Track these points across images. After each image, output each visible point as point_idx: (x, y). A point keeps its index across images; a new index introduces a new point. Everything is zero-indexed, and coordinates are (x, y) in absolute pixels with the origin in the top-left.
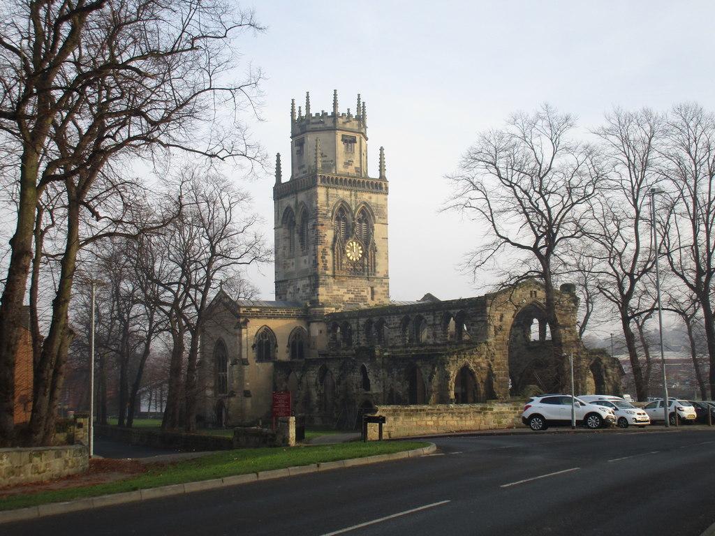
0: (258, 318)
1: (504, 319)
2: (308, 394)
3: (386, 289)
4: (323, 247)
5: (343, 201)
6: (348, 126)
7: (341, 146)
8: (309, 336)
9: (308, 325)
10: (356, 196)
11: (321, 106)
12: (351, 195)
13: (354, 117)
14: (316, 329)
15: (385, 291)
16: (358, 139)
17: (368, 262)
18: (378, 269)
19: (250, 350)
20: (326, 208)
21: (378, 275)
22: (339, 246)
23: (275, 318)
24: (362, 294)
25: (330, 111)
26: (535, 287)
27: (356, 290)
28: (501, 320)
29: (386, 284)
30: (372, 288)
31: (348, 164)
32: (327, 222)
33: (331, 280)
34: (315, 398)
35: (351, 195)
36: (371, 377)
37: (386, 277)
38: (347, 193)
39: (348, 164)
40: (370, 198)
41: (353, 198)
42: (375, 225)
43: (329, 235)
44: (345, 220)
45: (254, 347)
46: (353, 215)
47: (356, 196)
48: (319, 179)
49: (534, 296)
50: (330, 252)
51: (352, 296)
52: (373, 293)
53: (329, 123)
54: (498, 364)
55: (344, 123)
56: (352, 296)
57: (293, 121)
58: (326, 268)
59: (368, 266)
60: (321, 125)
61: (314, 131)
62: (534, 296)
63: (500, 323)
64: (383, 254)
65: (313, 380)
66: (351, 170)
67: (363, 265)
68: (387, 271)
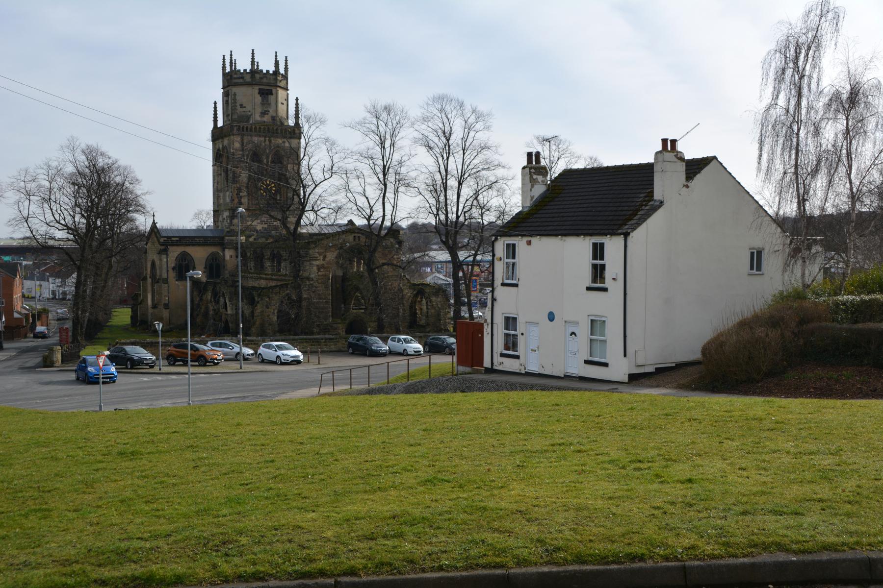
0: (177, 245)
1: (327, 259)
2: (207, 308)
6: (265, 80)
7: (258, 99)
8: (224, 259)
9: (223, 250)
10: (270, 141)
11: (244, 65)
13: (271, 72)
14: (228, 254)
16: (274, 92)
19: (171, 271)
22: (253, 186)
23: (193, 245)
25: (248, 69)
28: (324, 260)
31: (264, 113)
34: (211, 313)
36: (227, 301)
38: (262, 139)
39: (264, 113)
41: (267, 143)
43: (244, 176)
44: (260, 161)
45: (173, 269)
46: (267, 158)
47: (270, 141)
48: (235, 129)
49: (357, 240)
51: (266, 226)
54: (319, 295)
55: (261, 78)
56: (266, 226)
57: (225, 75)
60: (241, 80)
61: (236, 85)
62: (357, 240)
63: (322, 262)
65: (209, 297)
66: (266, 118)
67: (276, 199)
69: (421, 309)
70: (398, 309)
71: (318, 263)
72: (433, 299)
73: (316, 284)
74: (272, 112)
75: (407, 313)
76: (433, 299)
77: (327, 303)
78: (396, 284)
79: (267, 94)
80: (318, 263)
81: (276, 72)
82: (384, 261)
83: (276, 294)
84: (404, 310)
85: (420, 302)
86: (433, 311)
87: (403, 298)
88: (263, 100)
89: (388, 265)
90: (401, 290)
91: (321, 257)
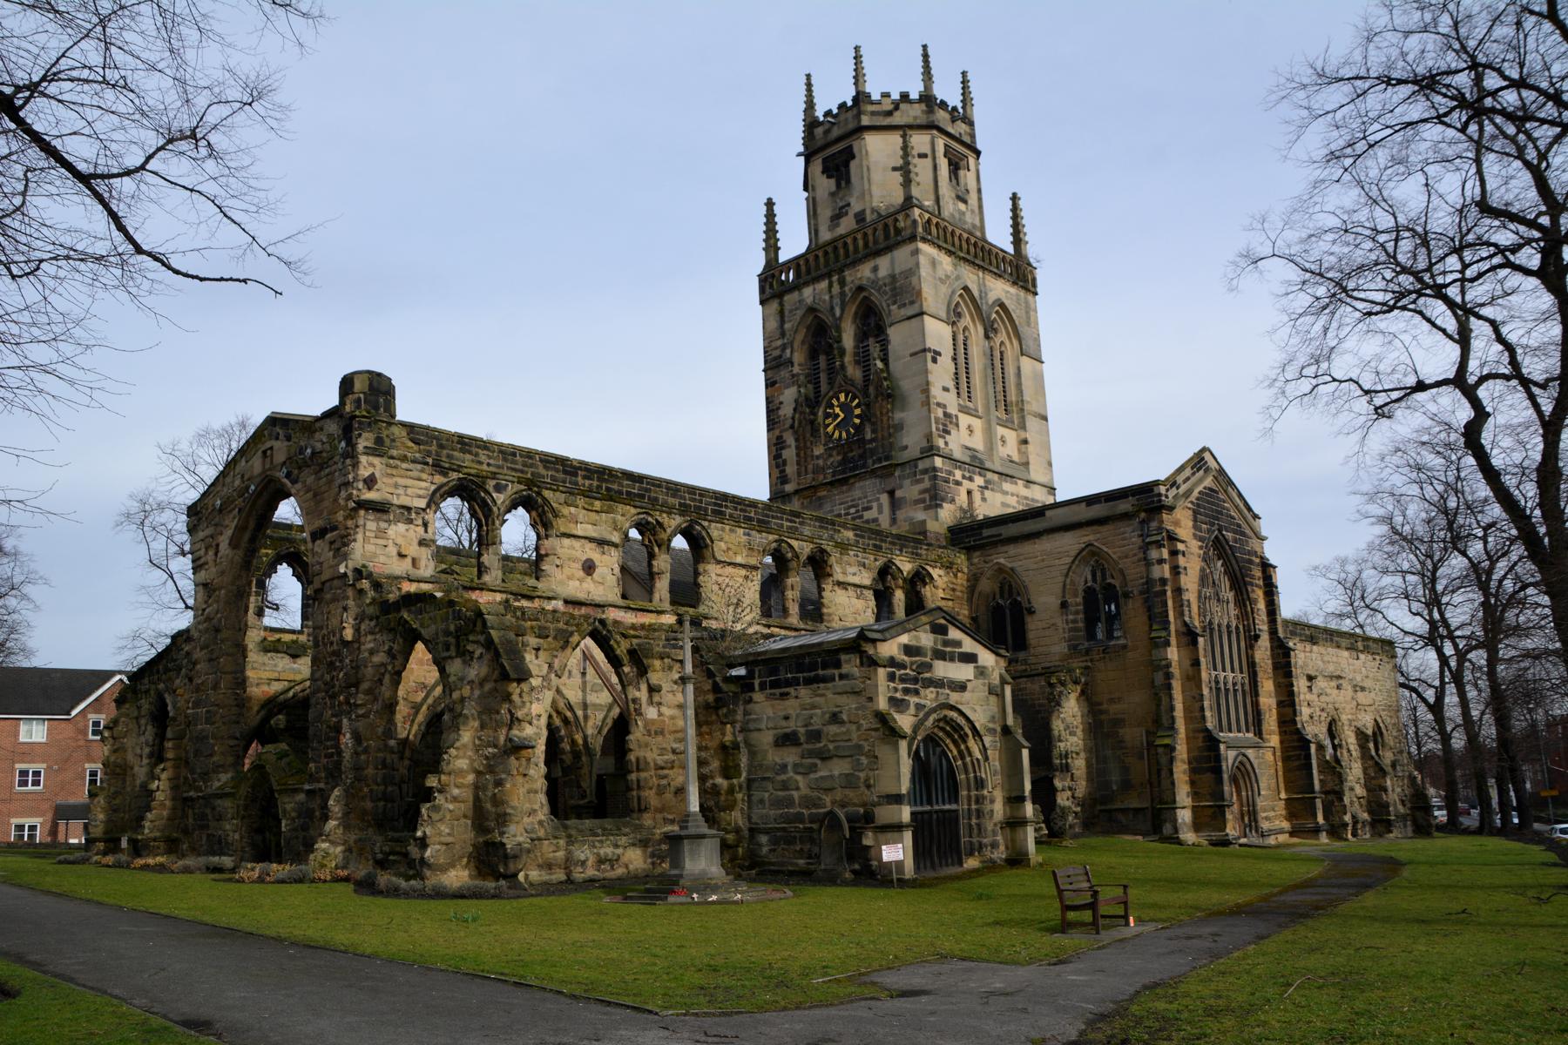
3: (927, 484)
4: (777, 432)
5: (811, 310)
12: (831, 285)
15: (925, 491)
17: (873, 431)
20: (779, 343)
24: (867, 515)
27: (852, 510)
29: (925, 471)
30: (891, 493)
32: (784, 373)
35: (831, 285)
40: (875, 269)
52: (895, 504)
59: (872, 440)
74: (856, 207)
79: (847, 165)
81: (861, 98)
88: (838, 186)
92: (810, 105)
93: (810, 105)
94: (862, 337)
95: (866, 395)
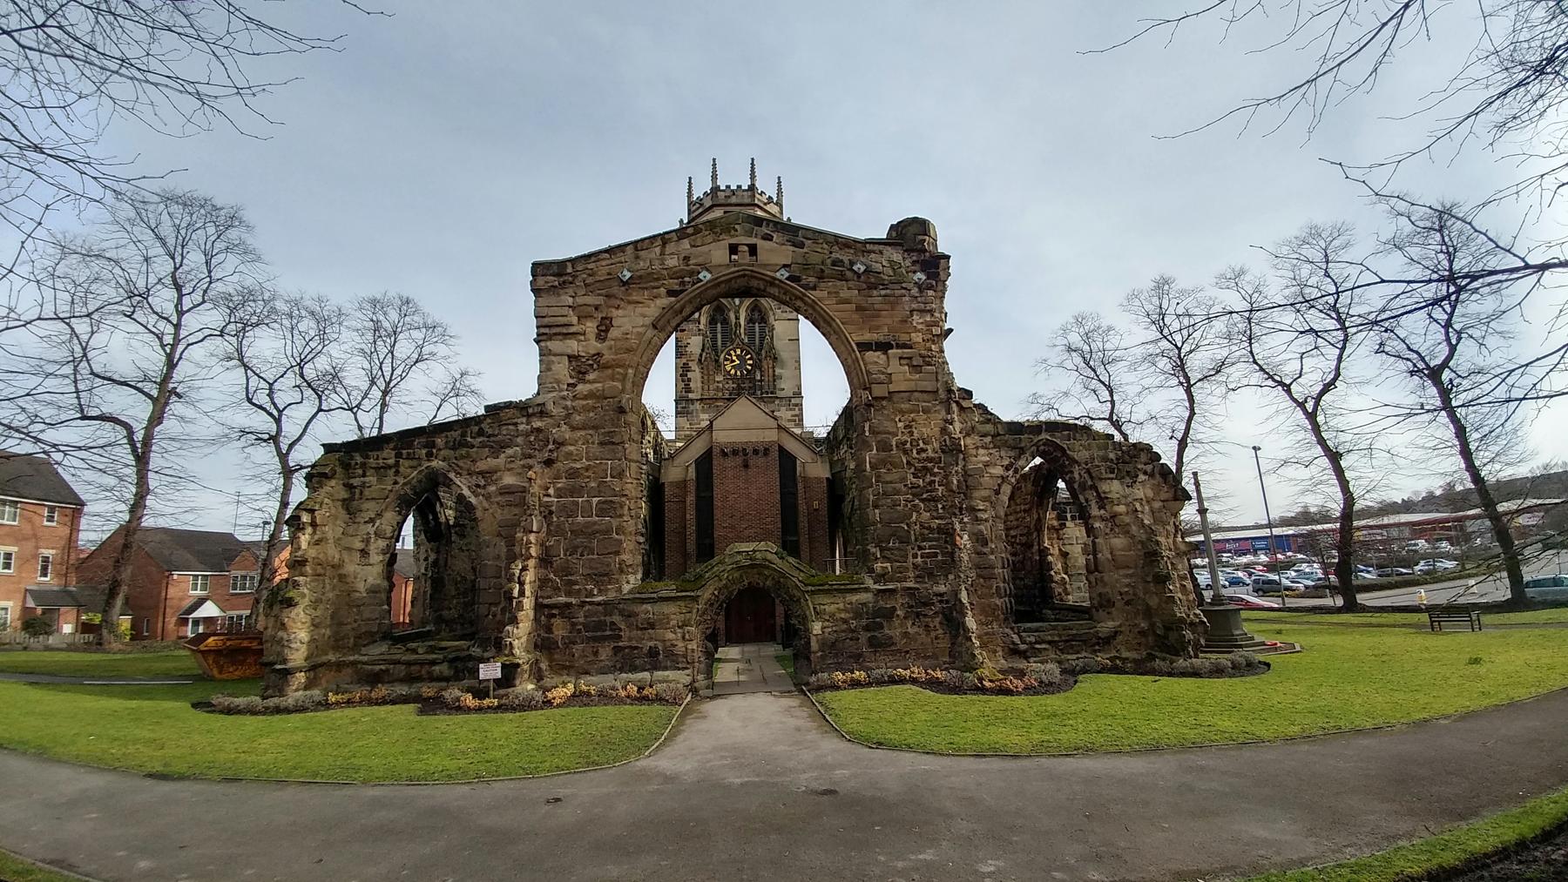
1: (613, 333)
6: (734, 200)
18: (782, 384)
21: (780, 394)
26: (750, 234)
33: (698, 405)
37: (798, 395)
42: (776, 324)
44: (725, 322)
50: (694, 366)
53: (708, 203)
54: (573, 474)
58: (688, 390)
63: (594, 346)
64: (791, 364)
68: (799, 387)
69: (1065, 555)
70: (948, 534)
71: (573, 346)
72: (1114, 488)
73: (564, 432)
75: (999, 553)
76: (1114, 488)
77: (608, 508)
78: (928, 428)
80: (573, 346)
81: (752, 188)
82: (867, 337)
83: (381, 470)
84: (980, 539)
85: (1058, 530)
86: (1119, 542)
87: (967, 488)
89: (884, 347)
90: (953, 450)
91: (591, 327)
92: (714, 177)
93: (714, 177)
94: (750, 321)
95: (759, 354)
